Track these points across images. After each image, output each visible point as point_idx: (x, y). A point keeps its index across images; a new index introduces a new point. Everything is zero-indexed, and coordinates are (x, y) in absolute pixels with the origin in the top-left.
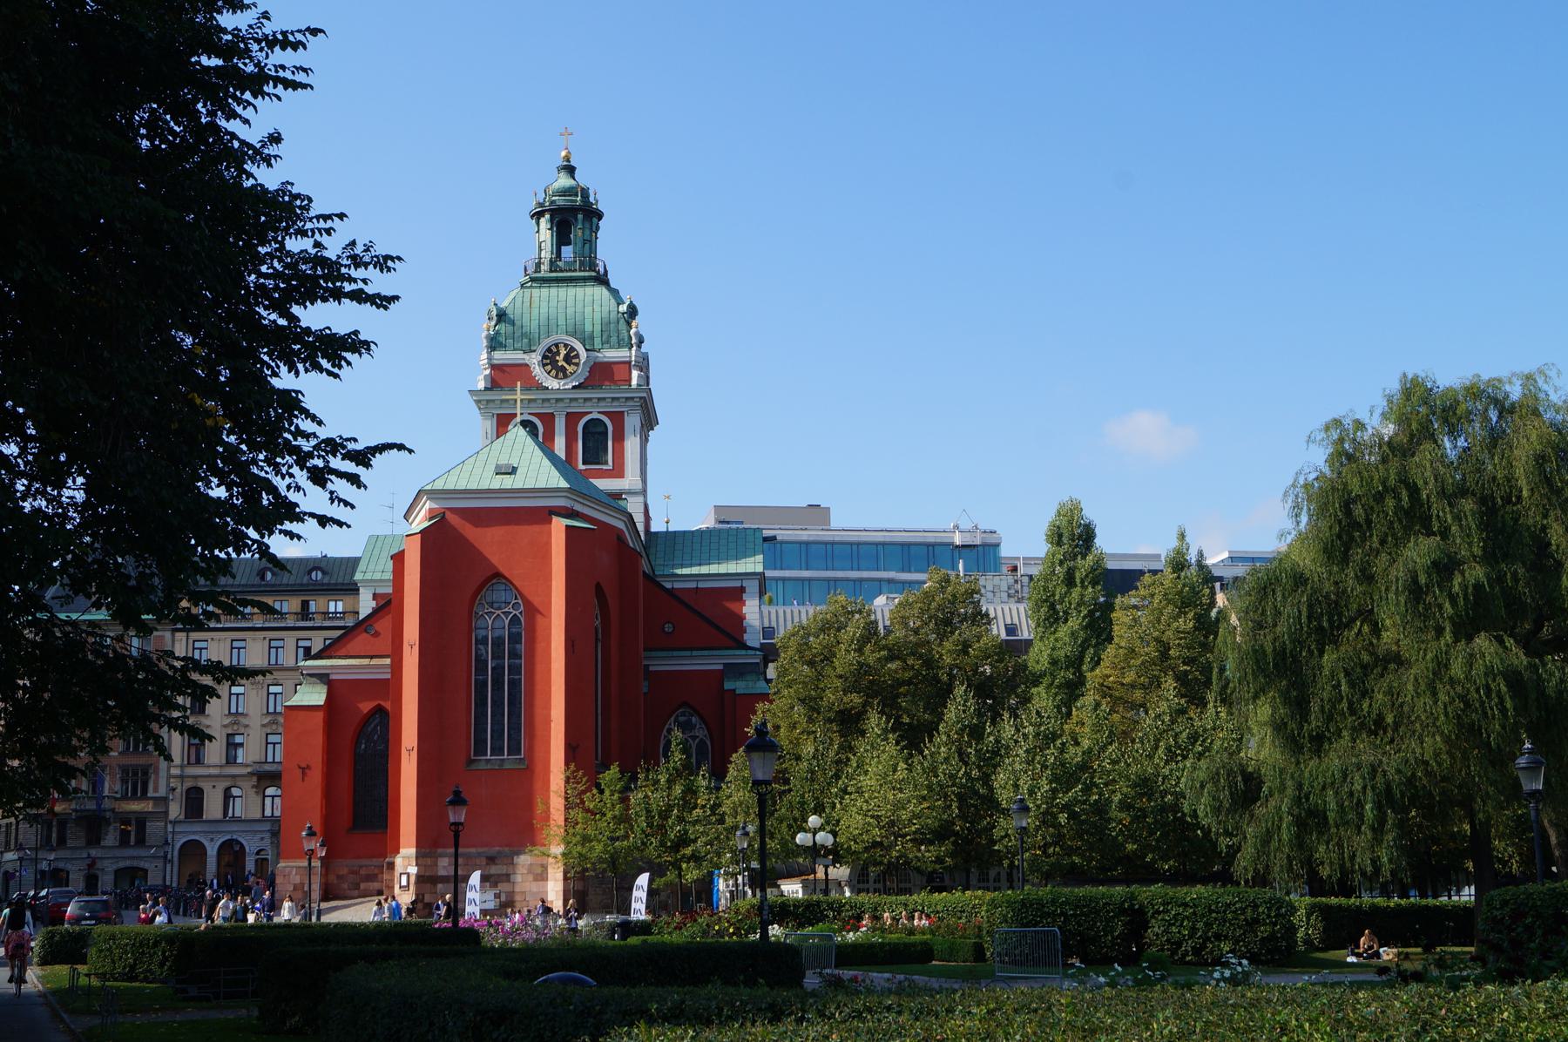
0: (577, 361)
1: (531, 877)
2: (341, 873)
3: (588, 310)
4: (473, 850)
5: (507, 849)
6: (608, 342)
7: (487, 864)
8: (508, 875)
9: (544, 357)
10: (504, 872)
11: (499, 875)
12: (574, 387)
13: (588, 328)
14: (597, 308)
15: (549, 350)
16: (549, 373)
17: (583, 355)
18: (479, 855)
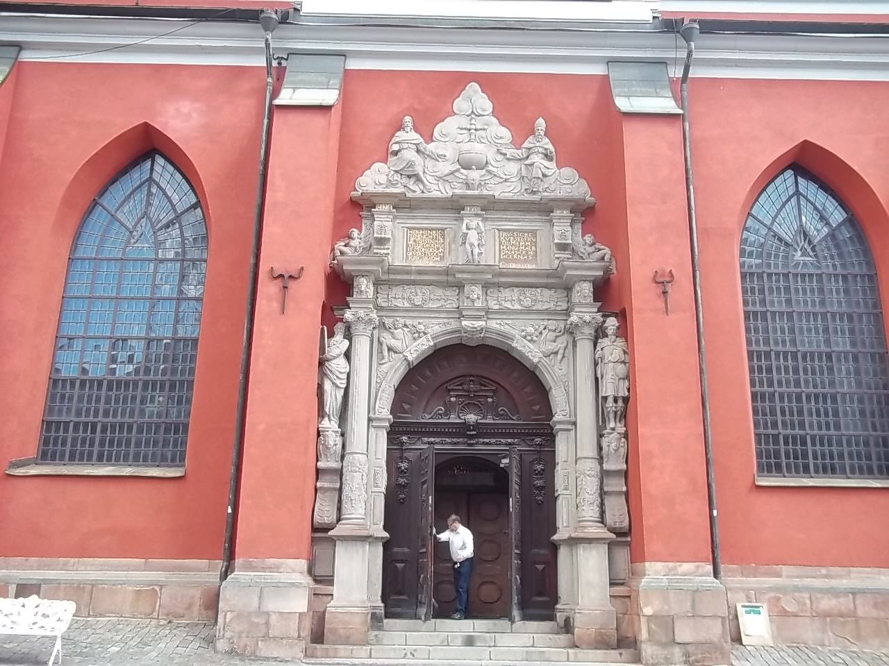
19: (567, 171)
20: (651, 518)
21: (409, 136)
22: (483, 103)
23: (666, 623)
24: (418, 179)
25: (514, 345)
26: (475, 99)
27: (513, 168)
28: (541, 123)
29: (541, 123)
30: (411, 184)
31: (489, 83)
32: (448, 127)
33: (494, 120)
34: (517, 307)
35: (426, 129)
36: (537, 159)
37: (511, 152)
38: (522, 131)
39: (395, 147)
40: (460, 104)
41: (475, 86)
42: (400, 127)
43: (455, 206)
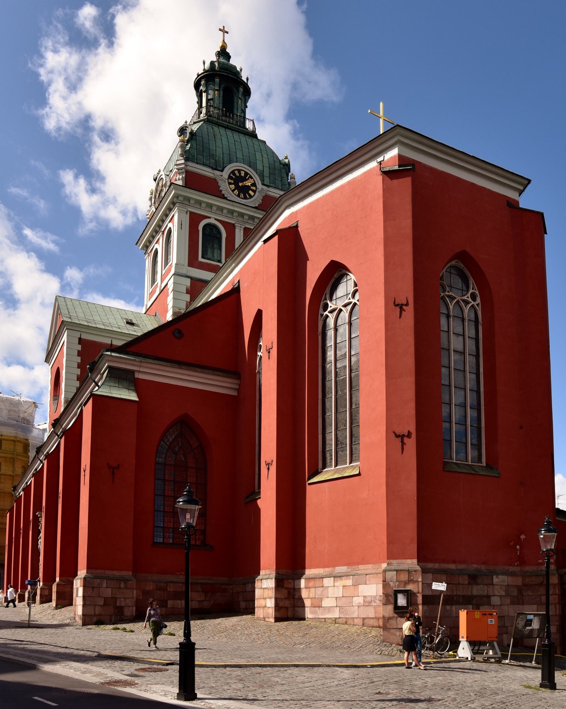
0: (254, 188)
1: (508, 601)
2: (147, 588)
3: (258, 155)
4: (452, 566)
5: (483, 567)
6: (275, 183)
7: (469, 583)
8: (488, 597)
9: (230, 177)
10: (485, 593)
11: (481, 597)
13: (260, 167)
14: (265, 156)
15: (233, 172)
16: (233, 191)
17: (260, 186)
18: (461, 572)
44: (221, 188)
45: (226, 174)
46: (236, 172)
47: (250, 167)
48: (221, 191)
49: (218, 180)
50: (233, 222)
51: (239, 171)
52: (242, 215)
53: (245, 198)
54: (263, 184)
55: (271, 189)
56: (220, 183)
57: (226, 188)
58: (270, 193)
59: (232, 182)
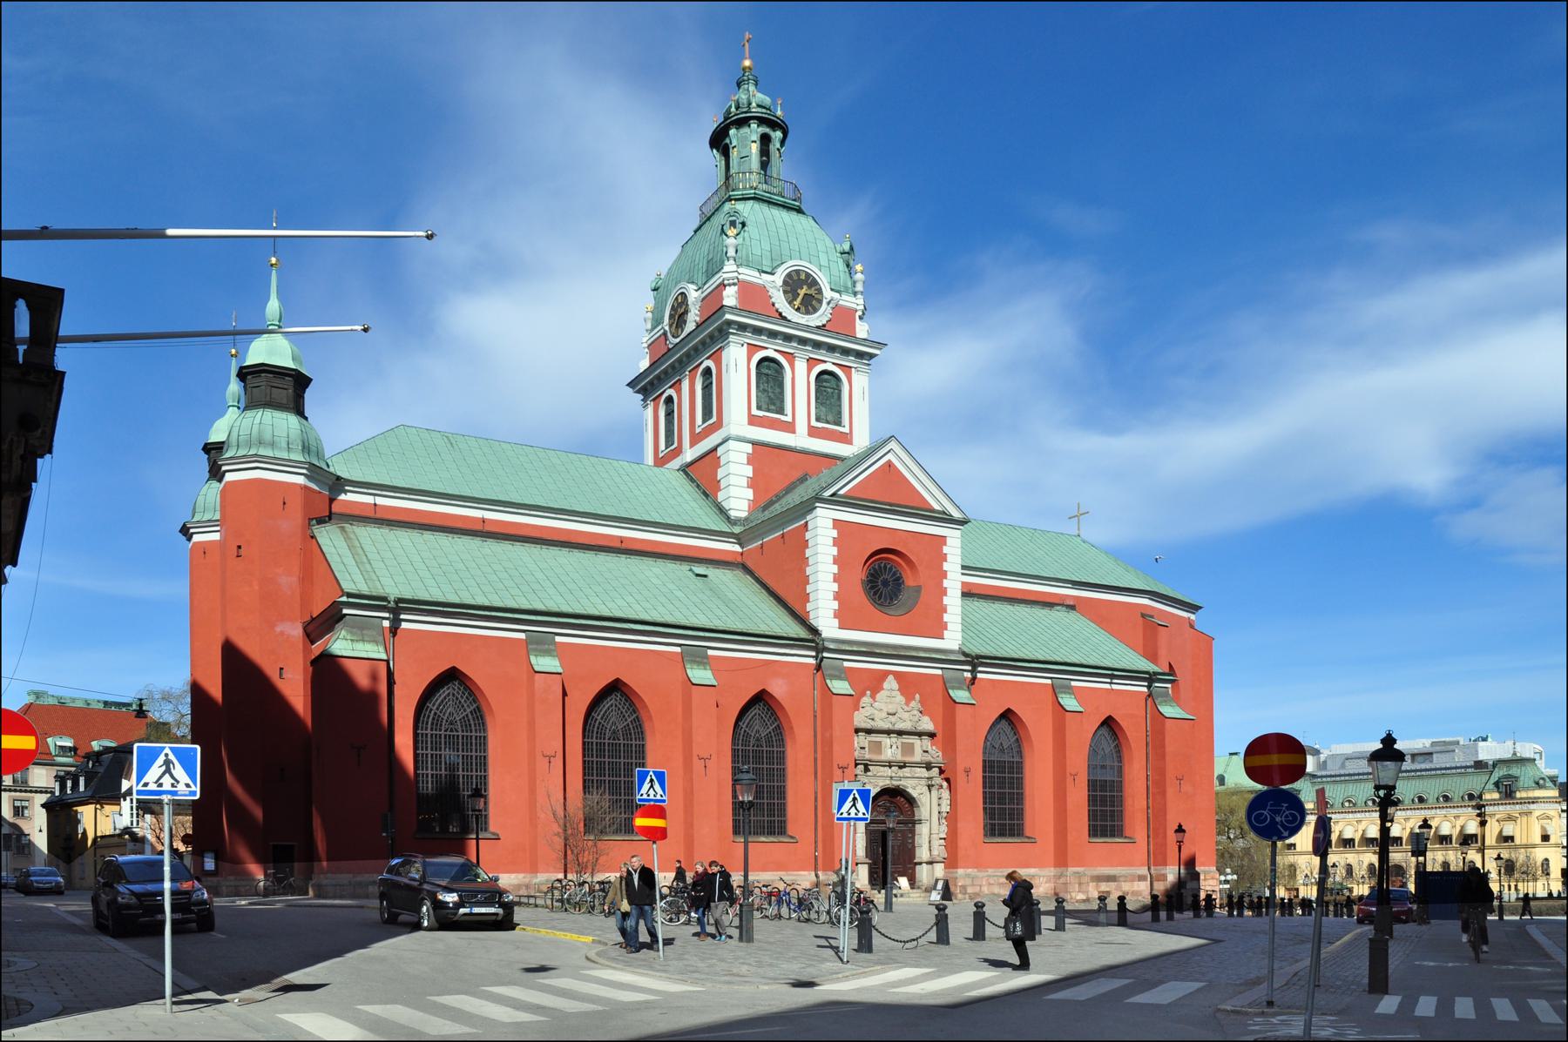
12: (818, 327)
17: (828, 294)
19: (926, 719)
20: (961, 853)
21: (866, 700)
22: (895, 685)
23: (964, 887)
24: (873, 719)
25: (908, 790)
26: (891, 684)
27: (905, 716)
28: (917, 696)
29: (917, 696)
30: (872, 723)
31: (896, 674)
32: (881, 696)
33: (898, 693)
34: (909, 775)
35: (873, 697)
36: (916, 712)
37: (906, 708)
38: (909, 699)
39: (864, 705)
40: (886, 685)
41: (891, 677)
42: (863, 694)
43: (888, 732)
44: (773, 300)
45: (779, 278)
46: (793, 274)
47: (810, 262)
48: (773, 305)
49: (768, 288)
50: (792, 351)
51: (797, 272)
52: (803, 341)
53: (807, 313)
54: (832, 290)
55: (844, 297)
56: (772, 292)
57: (780, 301)
58: (841, 302)
59: (789, 288)
